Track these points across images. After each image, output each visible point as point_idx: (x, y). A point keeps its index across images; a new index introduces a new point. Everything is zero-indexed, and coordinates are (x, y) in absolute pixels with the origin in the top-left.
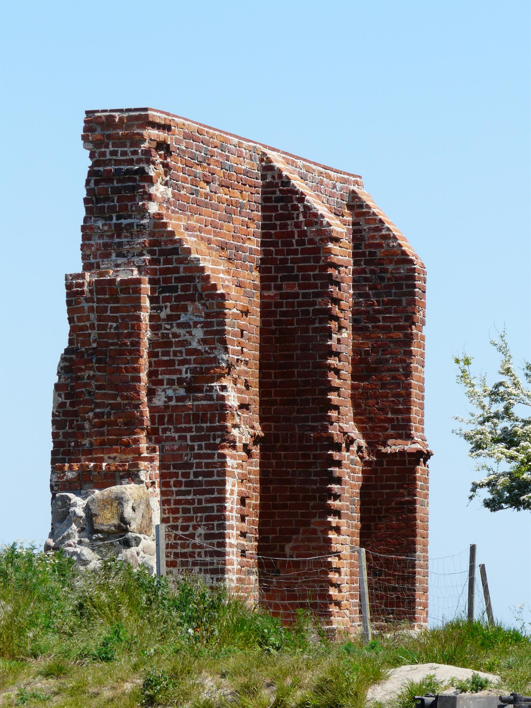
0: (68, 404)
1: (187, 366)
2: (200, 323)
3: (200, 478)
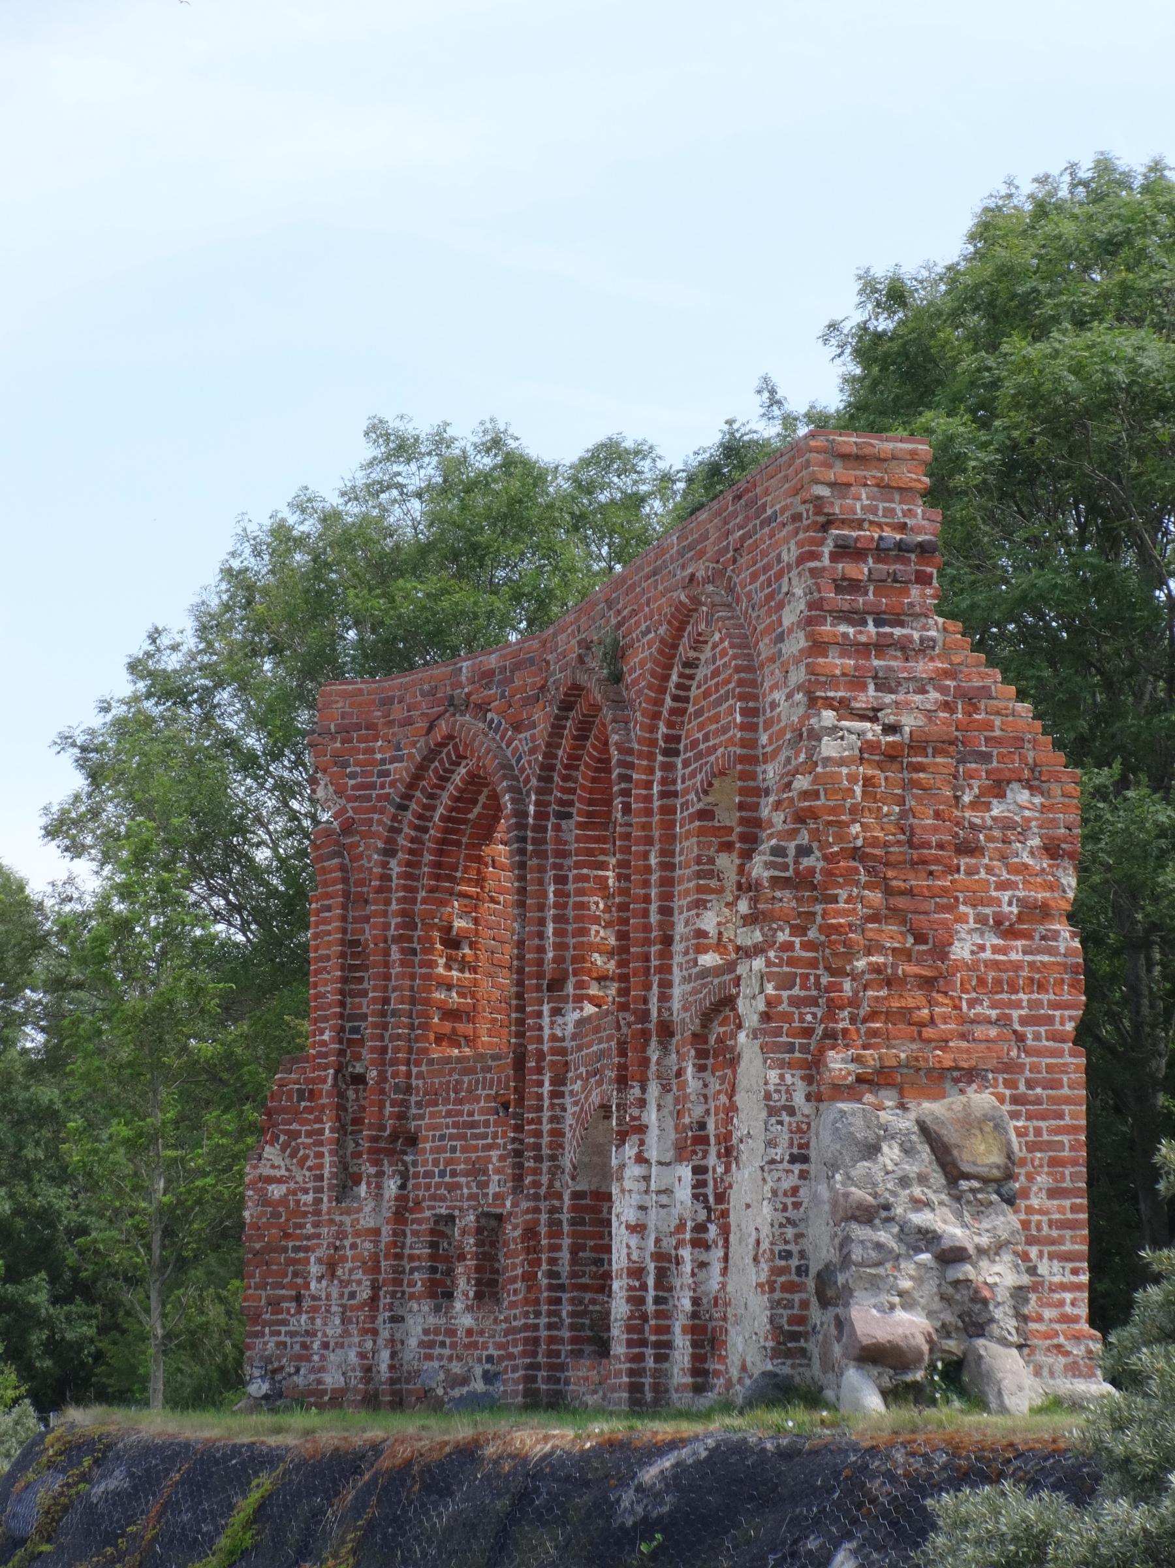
0: (798, 946)
1: (1009, 893)
2: (1037, 819)
3: (1039, 1090)
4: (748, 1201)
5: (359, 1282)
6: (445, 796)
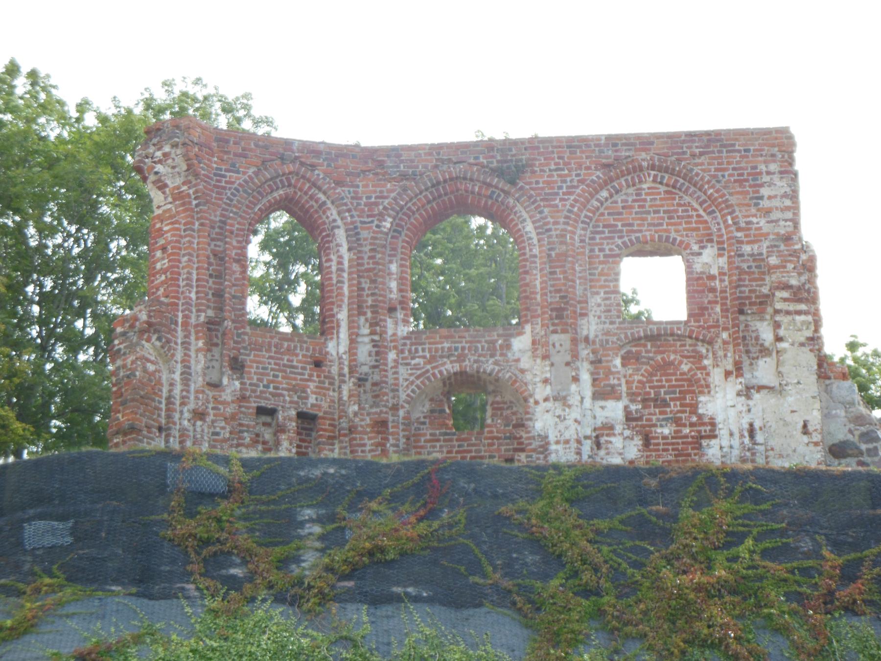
4: (794, 409)
5: (223, 428)
6: (265, 201)
